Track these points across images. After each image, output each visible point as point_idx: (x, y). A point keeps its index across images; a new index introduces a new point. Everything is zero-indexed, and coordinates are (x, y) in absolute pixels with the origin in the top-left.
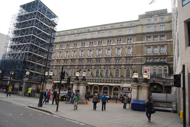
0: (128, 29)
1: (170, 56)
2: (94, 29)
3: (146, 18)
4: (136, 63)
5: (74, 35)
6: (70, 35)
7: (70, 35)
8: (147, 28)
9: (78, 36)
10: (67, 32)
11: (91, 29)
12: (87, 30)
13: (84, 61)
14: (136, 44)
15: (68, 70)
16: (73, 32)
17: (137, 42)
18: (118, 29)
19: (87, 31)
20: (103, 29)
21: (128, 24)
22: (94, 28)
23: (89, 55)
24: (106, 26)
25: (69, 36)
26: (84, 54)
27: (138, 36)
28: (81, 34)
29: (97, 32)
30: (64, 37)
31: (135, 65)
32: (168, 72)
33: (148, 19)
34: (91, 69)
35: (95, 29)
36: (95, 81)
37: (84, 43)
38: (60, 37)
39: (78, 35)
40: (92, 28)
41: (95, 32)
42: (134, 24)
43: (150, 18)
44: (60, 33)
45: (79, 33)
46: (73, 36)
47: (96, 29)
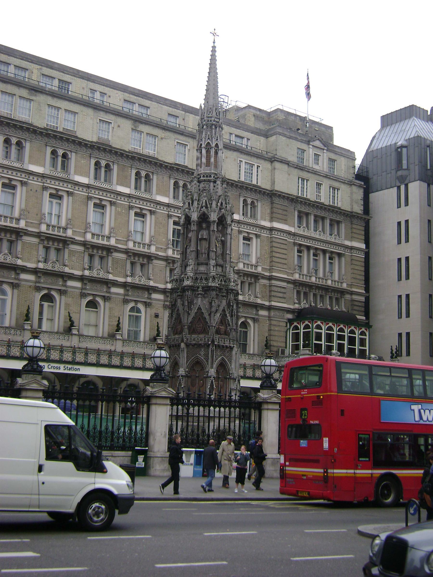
0: (244, 159)
1: (352, 293)
2: (93, 91)
3: (296, 139)
4: (273, 303)
14: (271, 229)
17: (276, 225)
19: (54, 86)
20: (136, 110)
21: (231, 134)
24: (147, 103)
27: (276, 200)
28: (41, 98)
29: (127, 124)
31: (269, 308)
32: (367, 348)
34: (106, 299)
35: (97, 95)
39: (24, 93)
40: (84, 83)
42: (248, 139)
43: (304, 146)
47: (103, 94)
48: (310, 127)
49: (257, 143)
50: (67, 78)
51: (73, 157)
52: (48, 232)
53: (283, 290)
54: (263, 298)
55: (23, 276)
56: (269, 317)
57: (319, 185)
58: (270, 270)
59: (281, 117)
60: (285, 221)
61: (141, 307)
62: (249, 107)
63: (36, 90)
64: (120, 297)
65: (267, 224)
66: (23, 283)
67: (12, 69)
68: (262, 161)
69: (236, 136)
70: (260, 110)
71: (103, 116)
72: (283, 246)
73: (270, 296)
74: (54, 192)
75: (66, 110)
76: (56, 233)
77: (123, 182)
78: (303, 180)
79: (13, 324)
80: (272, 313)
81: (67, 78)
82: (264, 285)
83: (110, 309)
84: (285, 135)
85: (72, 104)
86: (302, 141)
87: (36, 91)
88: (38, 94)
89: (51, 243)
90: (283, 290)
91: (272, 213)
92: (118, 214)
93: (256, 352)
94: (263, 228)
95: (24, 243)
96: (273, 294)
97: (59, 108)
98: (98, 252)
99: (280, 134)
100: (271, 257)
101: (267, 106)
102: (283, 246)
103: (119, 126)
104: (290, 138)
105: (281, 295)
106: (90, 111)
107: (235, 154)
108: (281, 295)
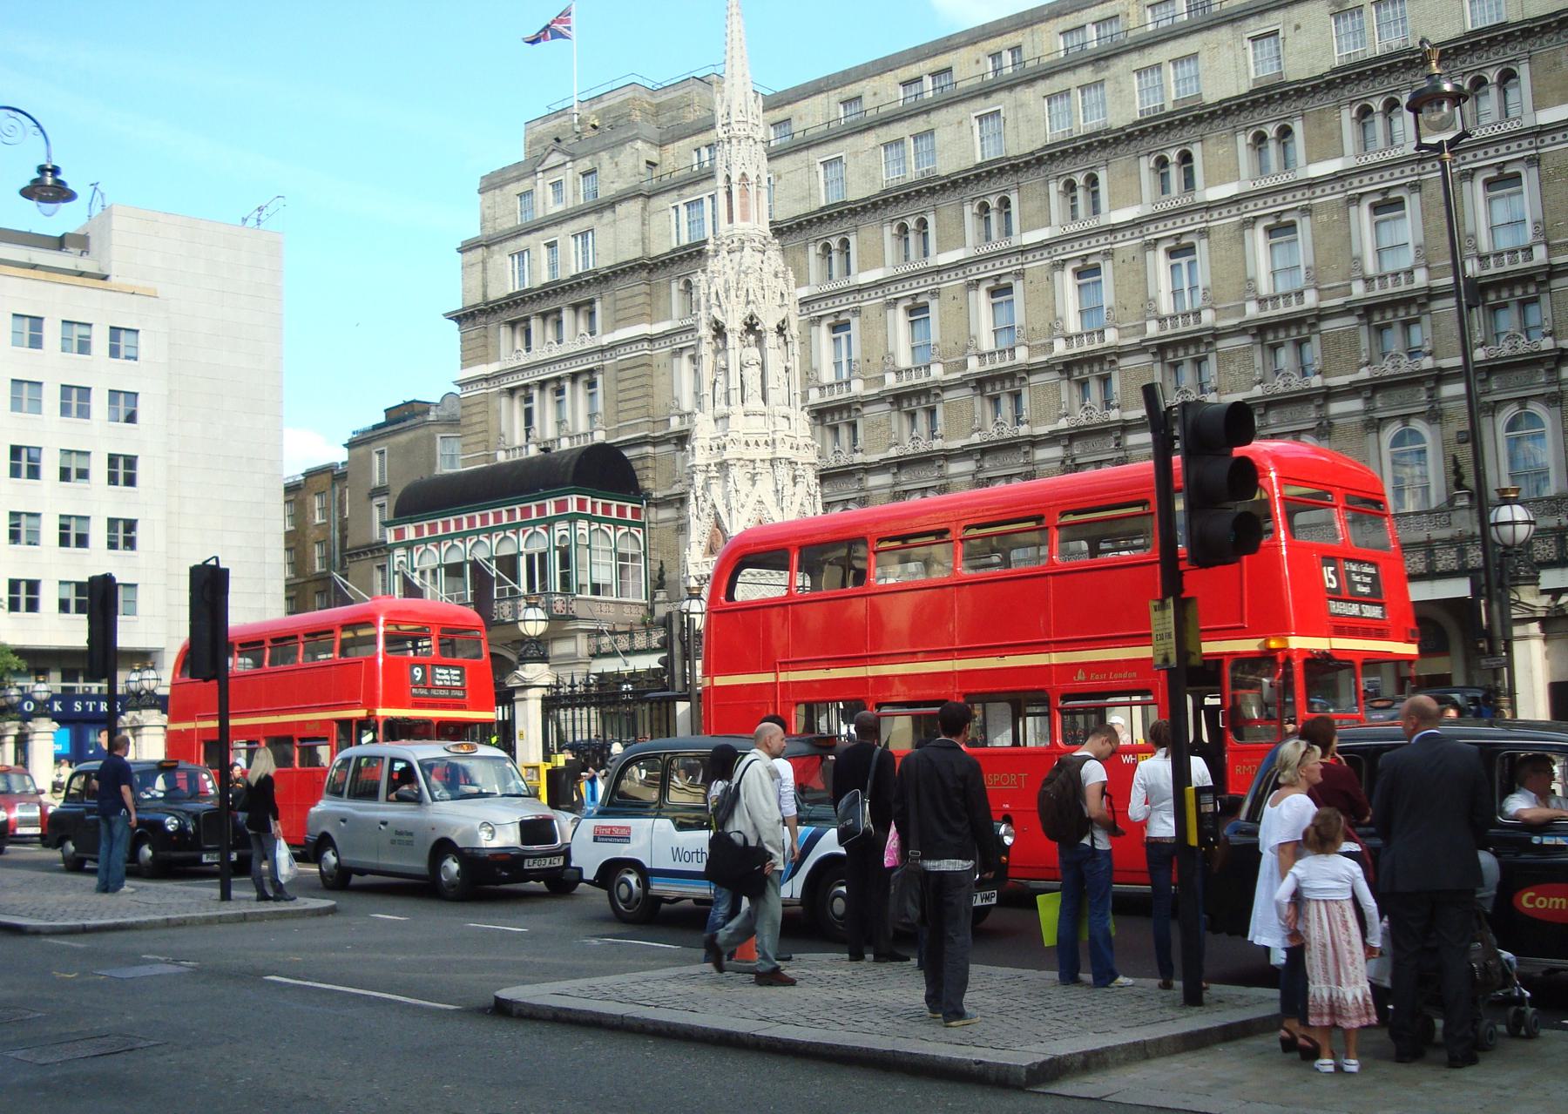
5: (1043, 87)
6: (985, 91)
7: (985, 91)
9: (1083, 88)
10: (941, 62)
13: (1225, 359)
23: (1370, 268)
26: (1203, 279)
28: (1121, 66)
30: (920, 124)
36: (1454, 566)
37: (1186, 158)
38: (870, 139)
39: (1086, 75)
44: (851, 91)
45: (1101, 59)
46: (1030, 96)
52: (1371, 294)
55: (1336, 408)
57: (551, 245)
61: (1418, 425)
64: (1355, 419)
66: (1134, 452)
67: (1092, 32)
74: (1493, 174)
75: (1175, 61)
76: (1391, 290)
77: (1325, 146)
85: (1182, 41)
87: (1107, 58)
88: (1111, 62)
89: (1086, 370)
95: (1125, 374)
97: (1158, 66)
98: (1512, 295)
103: (1297, 27)
106: (1225, 33)
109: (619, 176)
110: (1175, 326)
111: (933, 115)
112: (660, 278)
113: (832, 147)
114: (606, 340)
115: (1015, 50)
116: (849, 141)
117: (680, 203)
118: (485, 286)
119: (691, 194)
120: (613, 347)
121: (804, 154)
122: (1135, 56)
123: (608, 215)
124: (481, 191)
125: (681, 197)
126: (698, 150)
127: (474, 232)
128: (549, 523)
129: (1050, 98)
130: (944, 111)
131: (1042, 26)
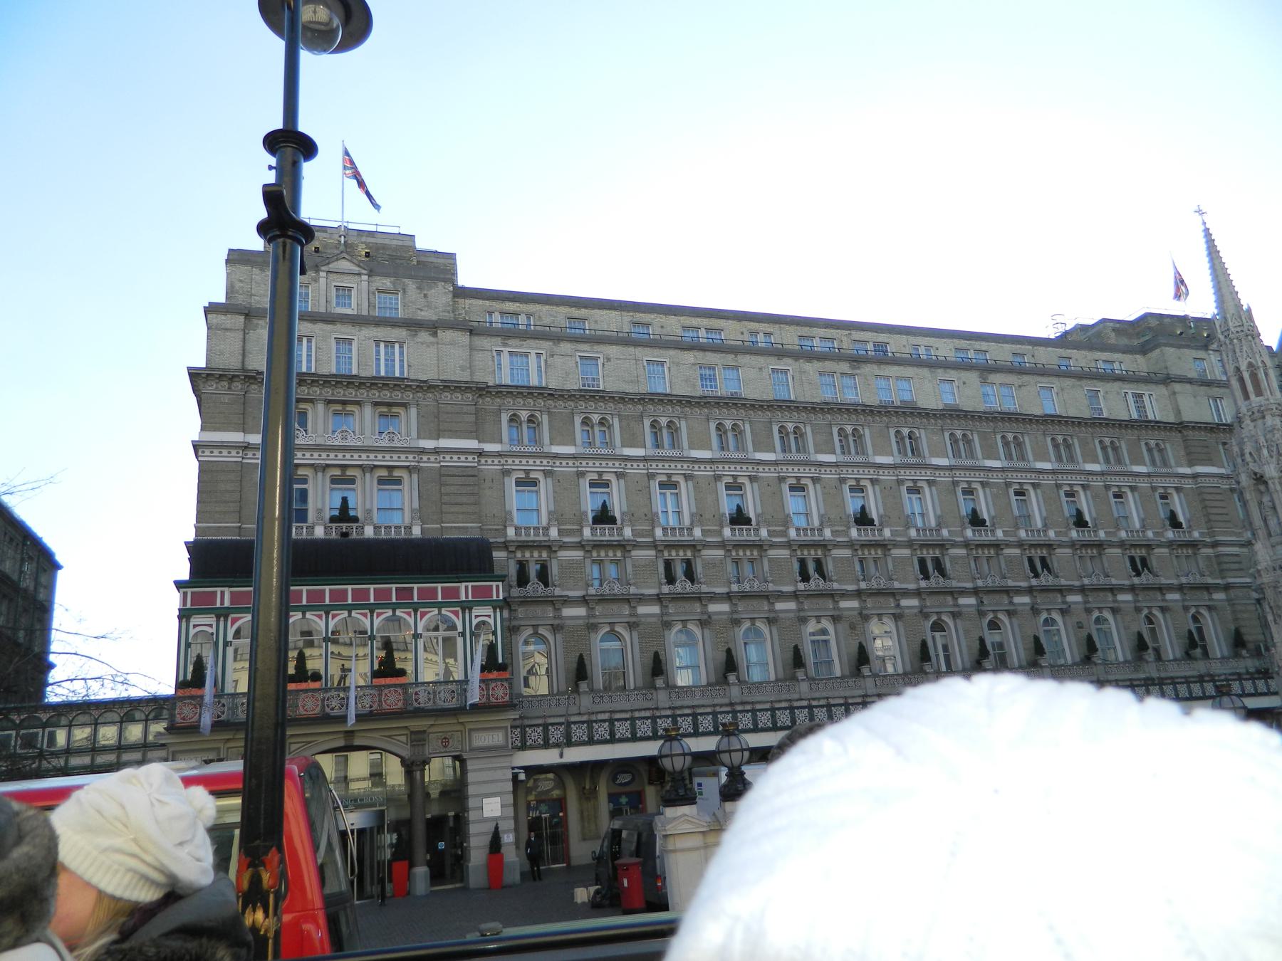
2: (916, 347)
5: (817, 365)
6: (780, 353)
8: (377, 343)
9: (842, 374)
11: (896, 345)
12: (870, 346)
14: (1195, 476)
15: (853, 627)
16: (761, 338)
17: (1200, 469)
18: (1084, 382)
22: (913, 340)
25: (773, 363)
28: (868, 369)
29: (973, 377)
31: (1227, 588)
33: (1195, 353)
39: (845, 367)
41: (966, 375)
43: (1201, 354)
44: (641, 317)
46: (811, 368)
48: (1196, 327)
49: (1138, 364)
50: (882, 338)
51: (922, 435)
53: (1236, 559)
54: (1211, 574)
56: (1229, 600)
58: (1212, 534)
59: (1154, 323)
60: (1210, 462)
62: (1104, 321)
63: (857, 360)
65: (1187, 471)
67: (816, 342)
68: (1153, 386)
69: (1104, 361)
70: (1119, 321)
71: (941, 374)
72: (1218, 497)
73: (1222, 571)
78: (1215, 399)
79: (908, 668)
80: (1232, 593)
81: (882, 338)
82: (1208, 557)
83: (1020, 626)
84: (1172, 346)
86: (1197, 348)
90: (1236, 559)
91: (1188, 454)
92: (995, 497)
93: (1226, 653)
94: (1184, 476)
96: (1225, 566)
99: (1166, 345)
100: (1207, 515)
101: (1129, 313)
102: (1218, 497)
104: (1180, 347)
105: (1236, 566)
106: (925, 372)
107: (1117, 385)
108: (1236, 566)
109: (429, 306)
110: (537, 534)
111: (740, 357)
112: (488, 403)
113: (657, 351)
114: (429, 444)
115: (768, 334)
116: (672, 352)
117: (506, 350)
118: (244, 355)
119: (515, 345)
120: (436, 451)
121: (631, 349)
122: (875, 367)
123: (424, 336)
124: (228, 262)
125: (505, 345)
126: (491, 313)
127: (221, 298)
128: (466, 607)
129: (821, 373)
130: (748, 357)
131: (787, 327)
